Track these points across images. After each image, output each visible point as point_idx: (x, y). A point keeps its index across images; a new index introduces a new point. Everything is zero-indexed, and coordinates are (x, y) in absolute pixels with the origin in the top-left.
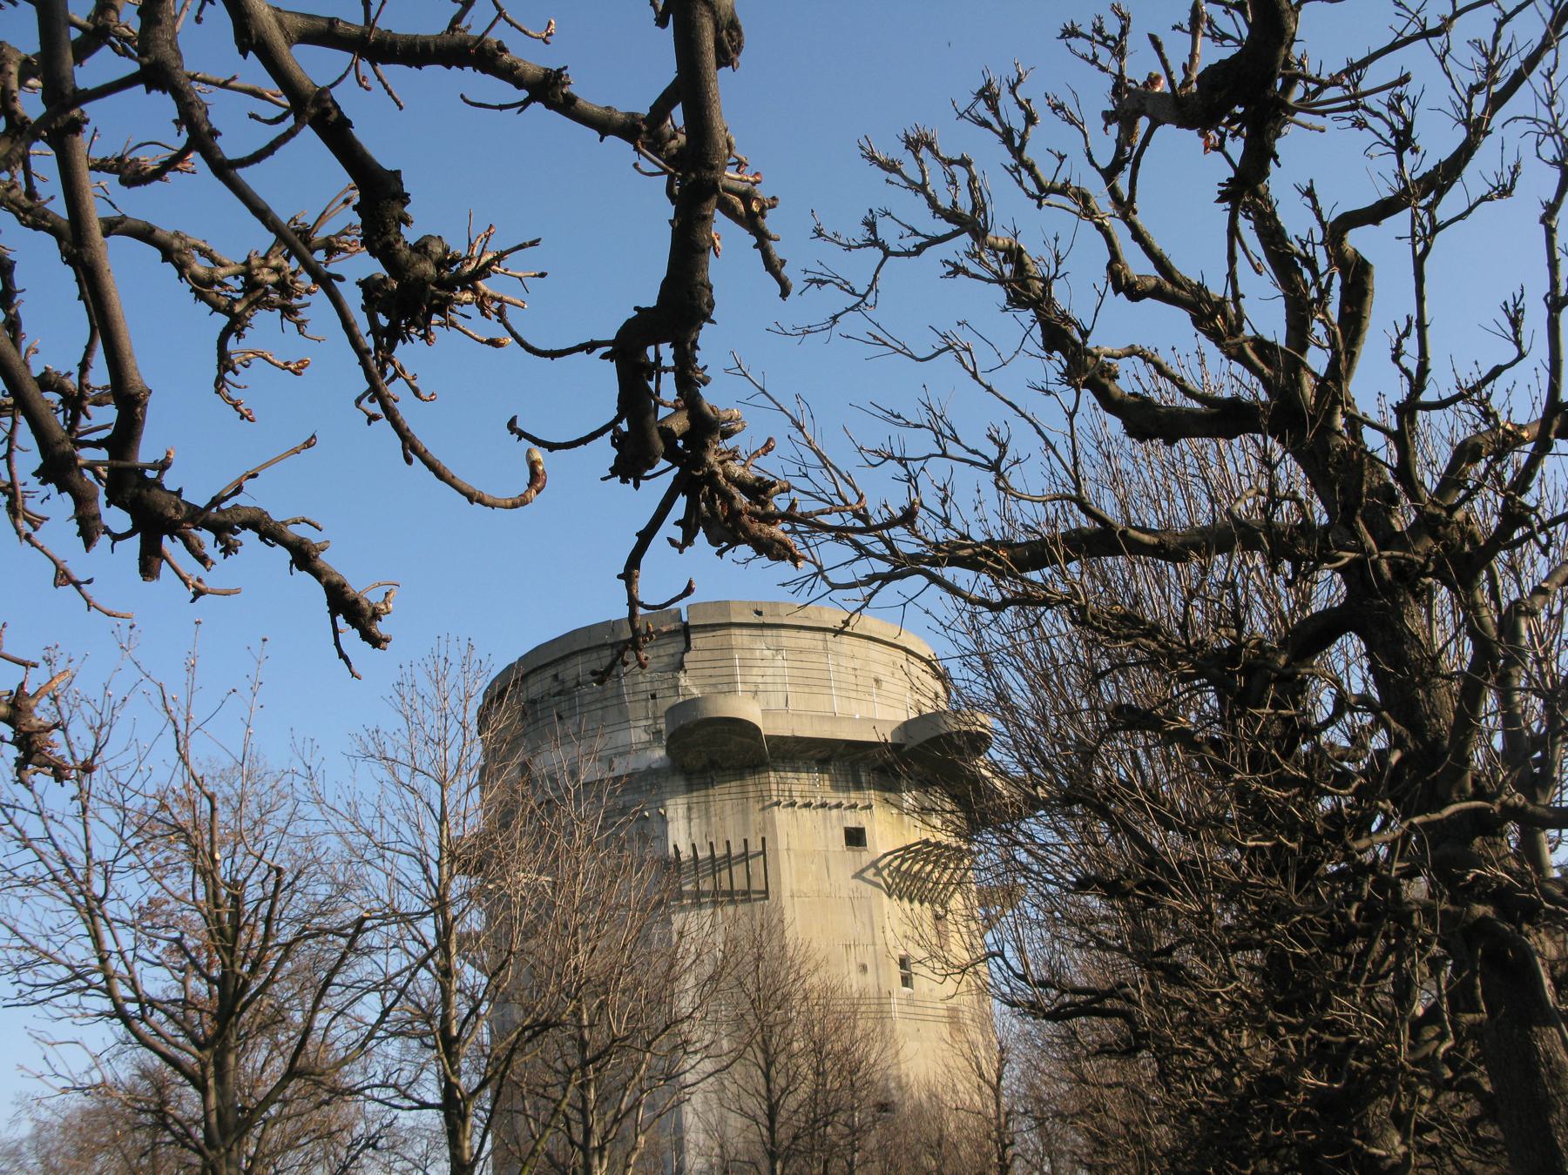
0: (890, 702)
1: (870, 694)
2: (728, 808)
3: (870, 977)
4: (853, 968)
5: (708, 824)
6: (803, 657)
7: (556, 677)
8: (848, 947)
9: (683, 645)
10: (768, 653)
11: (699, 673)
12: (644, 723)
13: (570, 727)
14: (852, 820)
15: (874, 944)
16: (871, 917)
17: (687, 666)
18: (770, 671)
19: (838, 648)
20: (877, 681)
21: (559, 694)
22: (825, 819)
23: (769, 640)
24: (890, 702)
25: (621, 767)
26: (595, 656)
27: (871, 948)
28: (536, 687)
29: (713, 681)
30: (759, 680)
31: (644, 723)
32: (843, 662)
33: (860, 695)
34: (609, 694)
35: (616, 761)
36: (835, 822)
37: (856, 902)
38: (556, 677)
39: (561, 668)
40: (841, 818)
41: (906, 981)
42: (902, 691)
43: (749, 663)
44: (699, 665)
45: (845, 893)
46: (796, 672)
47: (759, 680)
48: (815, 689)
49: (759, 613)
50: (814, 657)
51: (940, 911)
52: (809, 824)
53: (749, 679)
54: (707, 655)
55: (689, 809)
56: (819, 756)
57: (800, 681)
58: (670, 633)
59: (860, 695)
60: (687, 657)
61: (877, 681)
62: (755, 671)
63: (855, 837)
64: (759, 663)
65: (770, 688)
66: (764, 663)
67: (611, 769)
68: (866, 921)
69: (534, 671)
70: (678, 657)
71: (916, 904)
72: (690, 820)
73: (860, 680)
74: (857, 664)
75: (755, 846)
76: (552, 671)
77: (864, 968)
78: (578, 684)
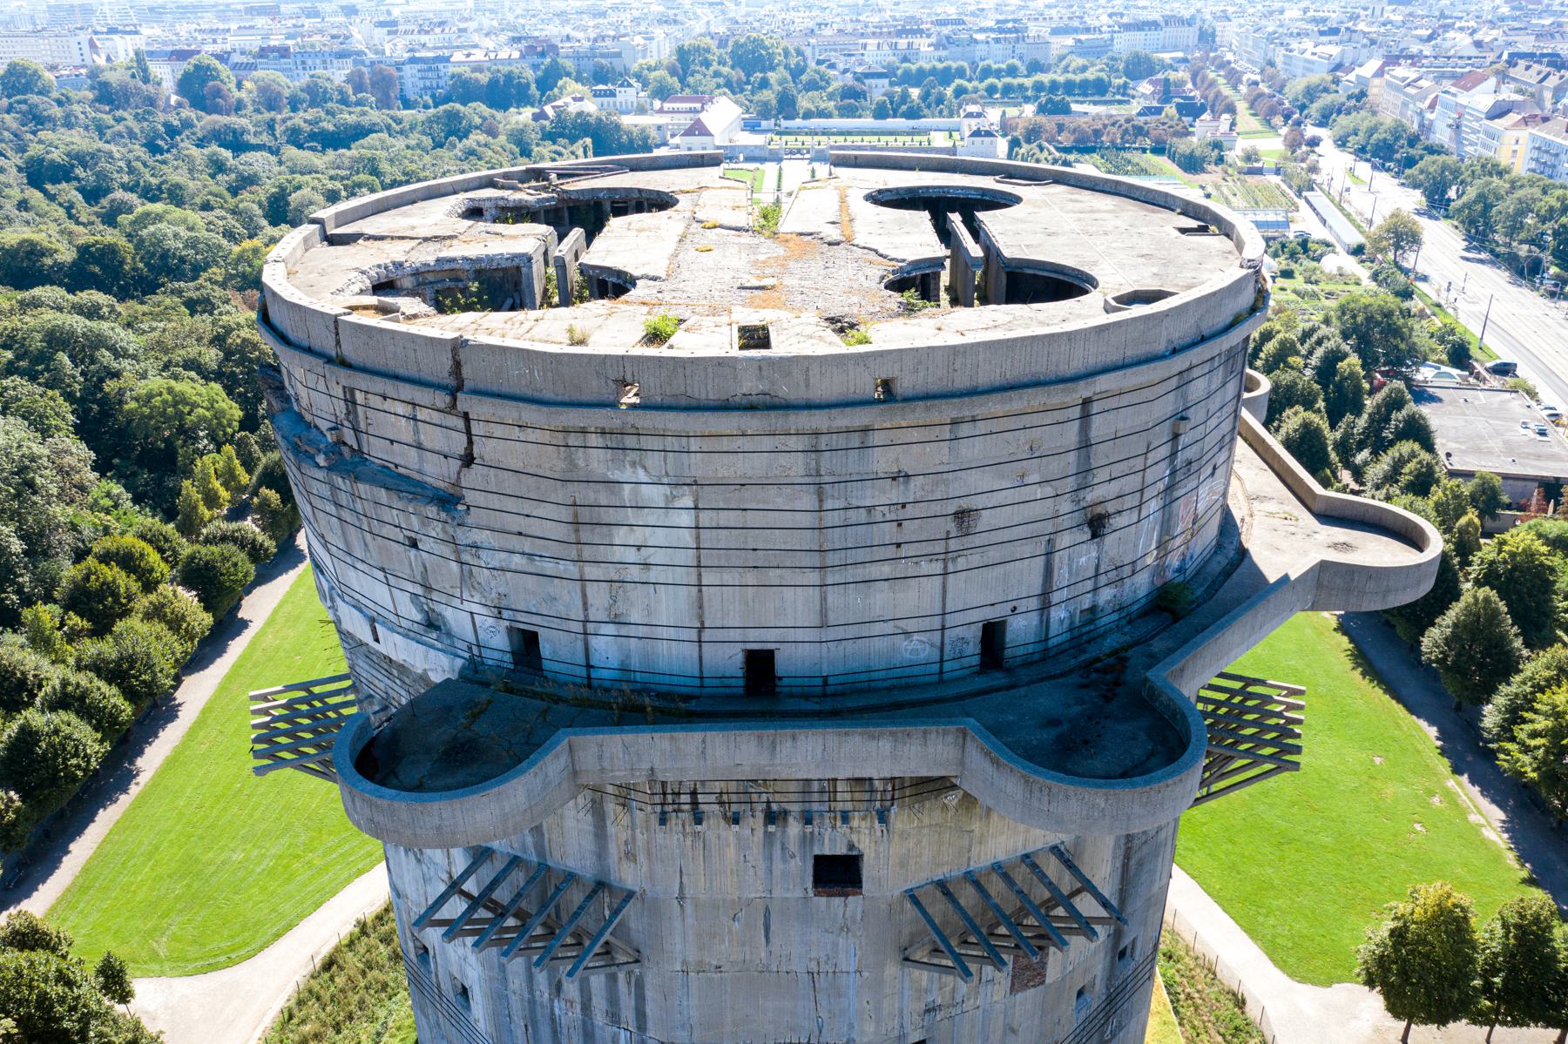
0: (994, 555)
6: (749, 497)
10: (655, 494)
14: (833, 843)
18: (659, 537)
23: (653, 460)
24: (994, 555)
29: (527, 545)
30: (631, 555)
36: (793, 846)
37: (822, 982)
45: (801, 969)
47: (631, 555)
48: (773, 576)
50: (776, 498)
52: (731, 853)
53: (602, 553)
54: (510, 483)
62: (620, 535)
63: (838, 874)
64: (631, 516)
65: (654, 575)
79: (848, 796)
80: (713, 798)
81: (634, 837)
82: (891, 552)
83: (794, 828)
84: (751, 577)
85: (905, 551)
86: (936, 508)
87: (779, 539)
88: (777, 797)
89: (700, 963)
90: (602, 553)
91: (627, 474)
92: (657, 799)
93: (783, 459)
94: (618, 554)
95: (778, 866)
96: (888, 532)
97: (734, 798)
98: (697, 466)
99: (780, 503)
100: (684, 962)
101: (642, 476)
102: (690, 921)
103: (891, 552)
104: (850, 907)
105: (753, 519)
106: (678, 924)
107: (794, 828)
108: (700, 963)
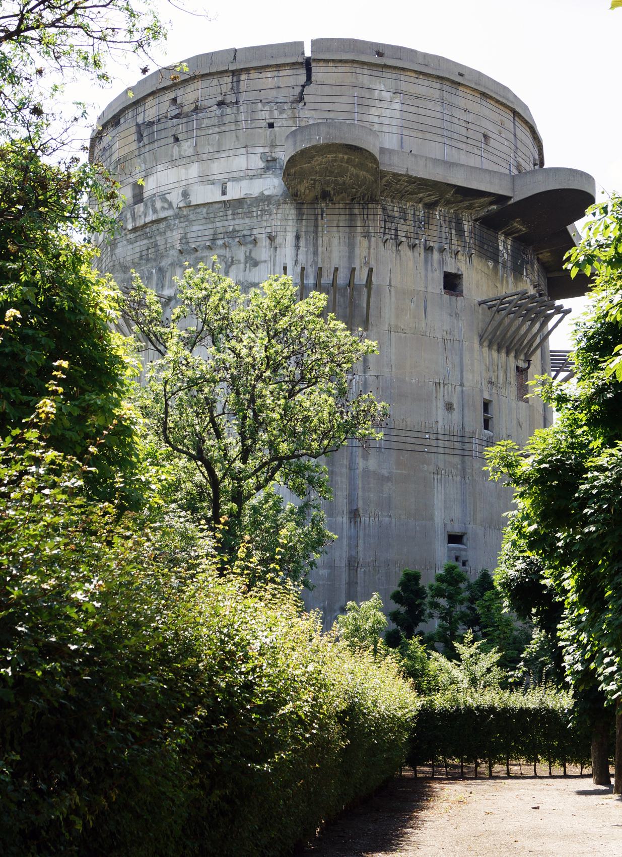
0: (495, 159)
1: (479, 148)
2: (335, 241)
3: (456, 415)
4: (441, 404)
5: (315, 253)
6: (419, 102)
7: (174, 100)
8: (437, 384)
9: (303, 79)
10: (387, 95)
11: (318, 106)
12: (261, 150)
13: (187, 147)
15: (462, 385)
16: (461, 359)
17: (306, 98)
18: (387, 113)
19: (453, 99)
20: (485, 136)
21: (176, 117)
22: (426, 261)
25: (235, 192)
26: (215, 82)
27: (458, 388)
28: (151, 111)
30: (376, 120)
31: (261, 150)
32: (458, 113)
33: (470, 149)
34: (227, 119)
35: (229, 185)
36: (436, 265)
38: (174, 100)
39: (179, 92)
40: (442, 263)
41: (487, 424)
42: (507, 150)
43: (367, 102)
44: (319, 99)
46: (411, 117)
47: (376, 120)
48: (428, 136)
49: (380, 54)
50: (430, 105)
51: (522, 364)
52: (411, 264)
53: (365, 117)
54: (327, 90)
55: (298, 238)
56: (427, 200)
57: (415, 126)
58: (293, 65)
59: (470, 149)
60: (307, 90)
61: (485, 136)
62: (373, 111)
63: (452, 283)
64: (377, 103)
65: (385, 128)
66: (382, 104)
67: (224, 193)
68: (457, 360)
69: (153, 93)
70: (298, 90)
71: (503, 355)
72: (297, 247)
73: (471, 134)
74: (470, 117)
75: (361, 277)
76: (171, 95)
77: (449, 407)
78: (196, 109)
79: (456, 242)
80: (404, 234)
81: (369, 253)
82: (465, 139)
83: (436, 255)
84: (420, 135)
85: (469, 141)
86: (478, 129)
87: (429, 121)
88: (429, 238)
89: (396, 326)
90: (365, 117)
91: (377, 87)
92: (382, 230)
93: (431, 90)
94: (371, 119)
95: (430, 274)
96: (463, 131)
97: (412, 235)
98: (404, 86)
99: (430, 107)
100: (390, 325)
101: (382, 88)
102: (393, 299)
103: (465, 139)
104: (459, 302)
105: (421, 111)
106: (387, 300)
107: (436, 255)
108: (396, 326)
